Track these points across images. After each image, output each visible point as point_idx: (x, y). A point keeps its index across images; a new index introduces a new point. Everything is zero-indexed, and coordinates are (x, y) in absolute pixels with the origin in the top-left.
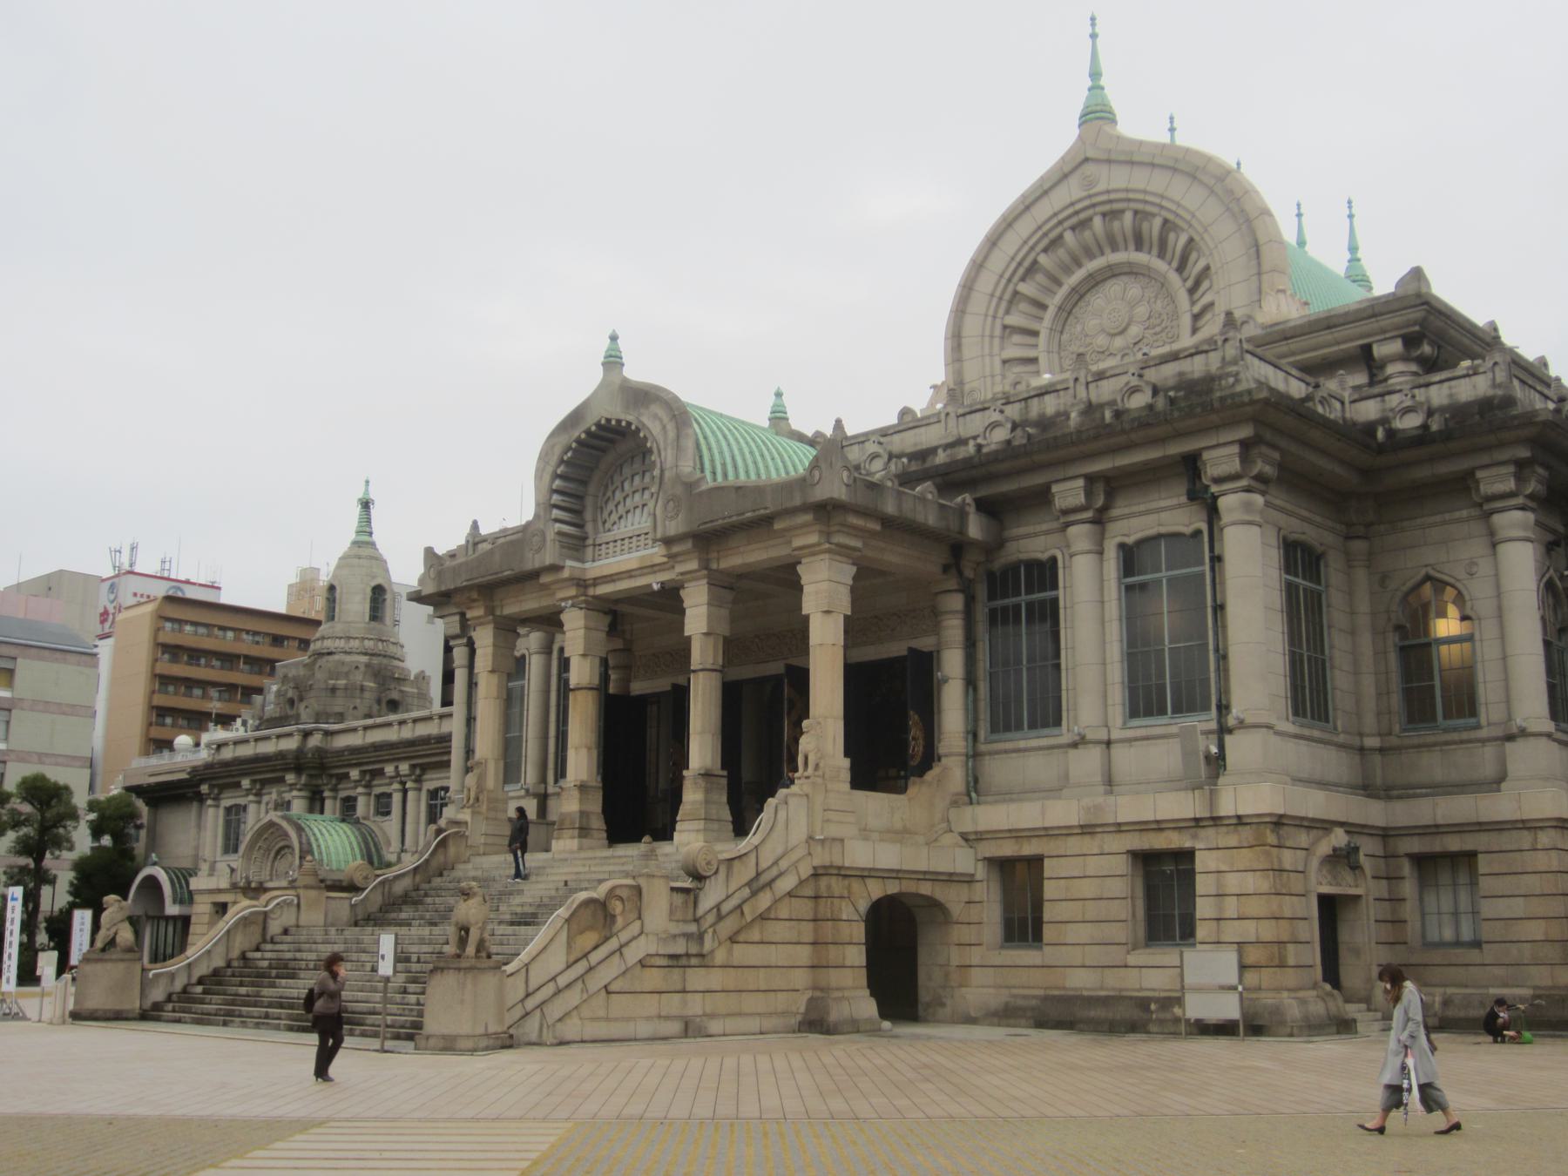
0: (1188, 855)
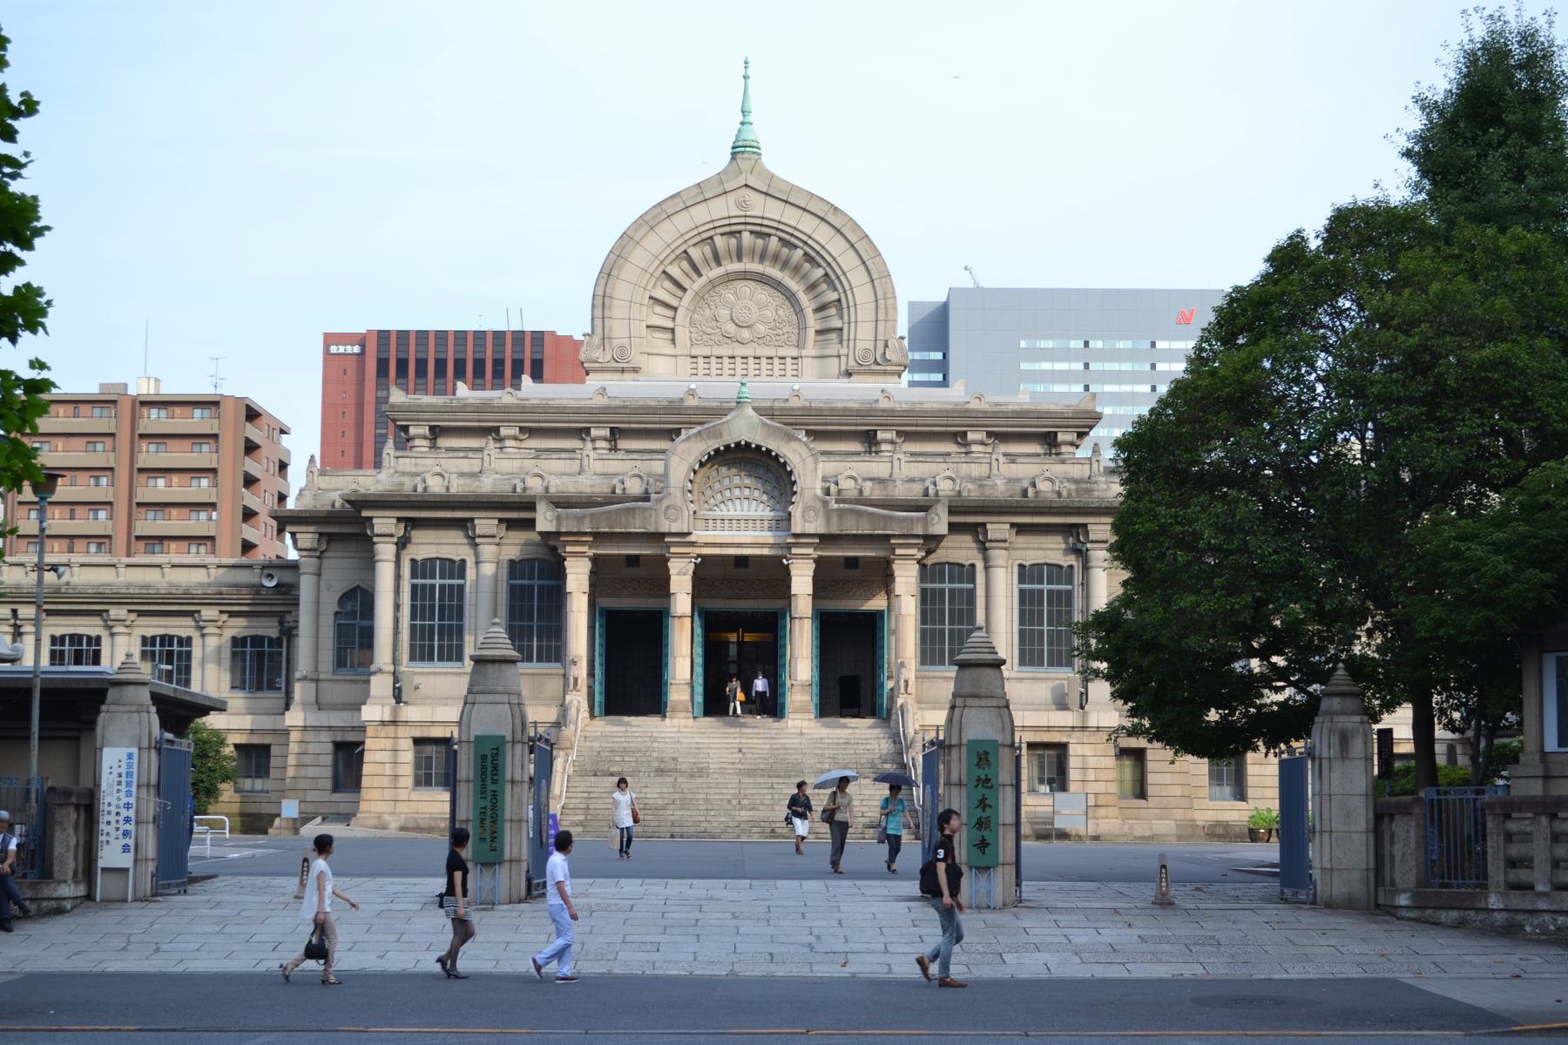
0: (1062, 748)
